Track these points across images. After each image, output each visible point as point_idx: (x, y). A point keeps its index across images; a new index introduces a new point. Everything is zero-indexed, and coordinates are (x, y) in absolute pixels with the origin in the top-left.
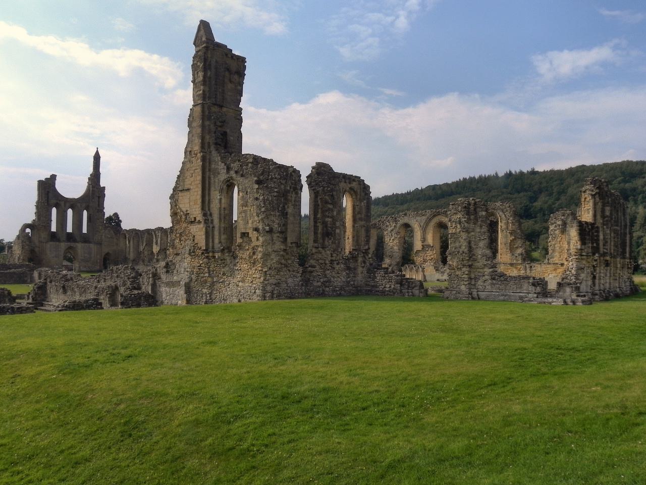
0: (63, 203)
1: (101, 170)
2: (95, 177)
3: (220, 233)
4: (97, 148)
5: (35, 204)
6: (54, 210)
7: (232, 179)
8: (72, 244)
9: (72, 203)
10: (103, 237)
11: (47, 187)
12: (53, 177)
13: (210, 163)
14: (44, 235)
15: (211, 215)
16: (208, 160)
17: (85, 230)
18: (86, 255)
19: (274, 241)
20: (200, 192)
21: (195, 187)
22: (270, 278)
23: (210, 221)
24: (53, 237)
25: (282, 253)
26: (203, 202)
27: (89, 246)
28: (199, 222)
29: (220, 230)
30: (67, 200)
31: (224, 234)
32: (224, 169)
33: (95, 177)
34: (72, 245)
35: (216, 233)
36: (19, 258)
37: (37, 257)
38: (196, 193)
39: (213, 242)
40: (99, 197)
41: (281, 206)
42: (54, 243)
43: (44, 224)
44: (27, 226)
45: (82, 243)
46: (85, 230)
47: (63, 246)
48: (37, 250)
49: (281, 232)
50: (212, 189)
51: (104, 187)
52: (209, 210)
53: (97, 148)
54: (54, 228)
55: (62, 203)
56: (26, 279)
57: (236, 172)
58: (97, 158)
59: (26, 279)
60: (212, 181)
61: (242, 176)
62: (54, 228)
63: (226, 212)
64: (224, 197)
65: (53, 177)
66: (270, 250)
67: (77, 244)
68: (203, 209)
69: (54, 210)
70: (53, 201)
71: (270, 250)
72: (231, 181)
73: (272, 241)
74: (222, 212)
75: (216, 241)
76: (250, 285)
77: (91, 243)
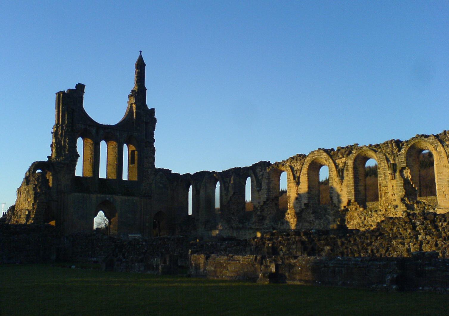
2: (139, 94)
4: (141, 52)
5: (52, 130)
8: (108, 197)
10: (153, 186)
11: (70, 102)
12: (80, 88)
33: (139, 94)
36: (28, 217)
40: (147, 123)
51: (153, 109)
53: (141, 52)
54: (79, 172)
58: (141, 66)
65: (80, 88)
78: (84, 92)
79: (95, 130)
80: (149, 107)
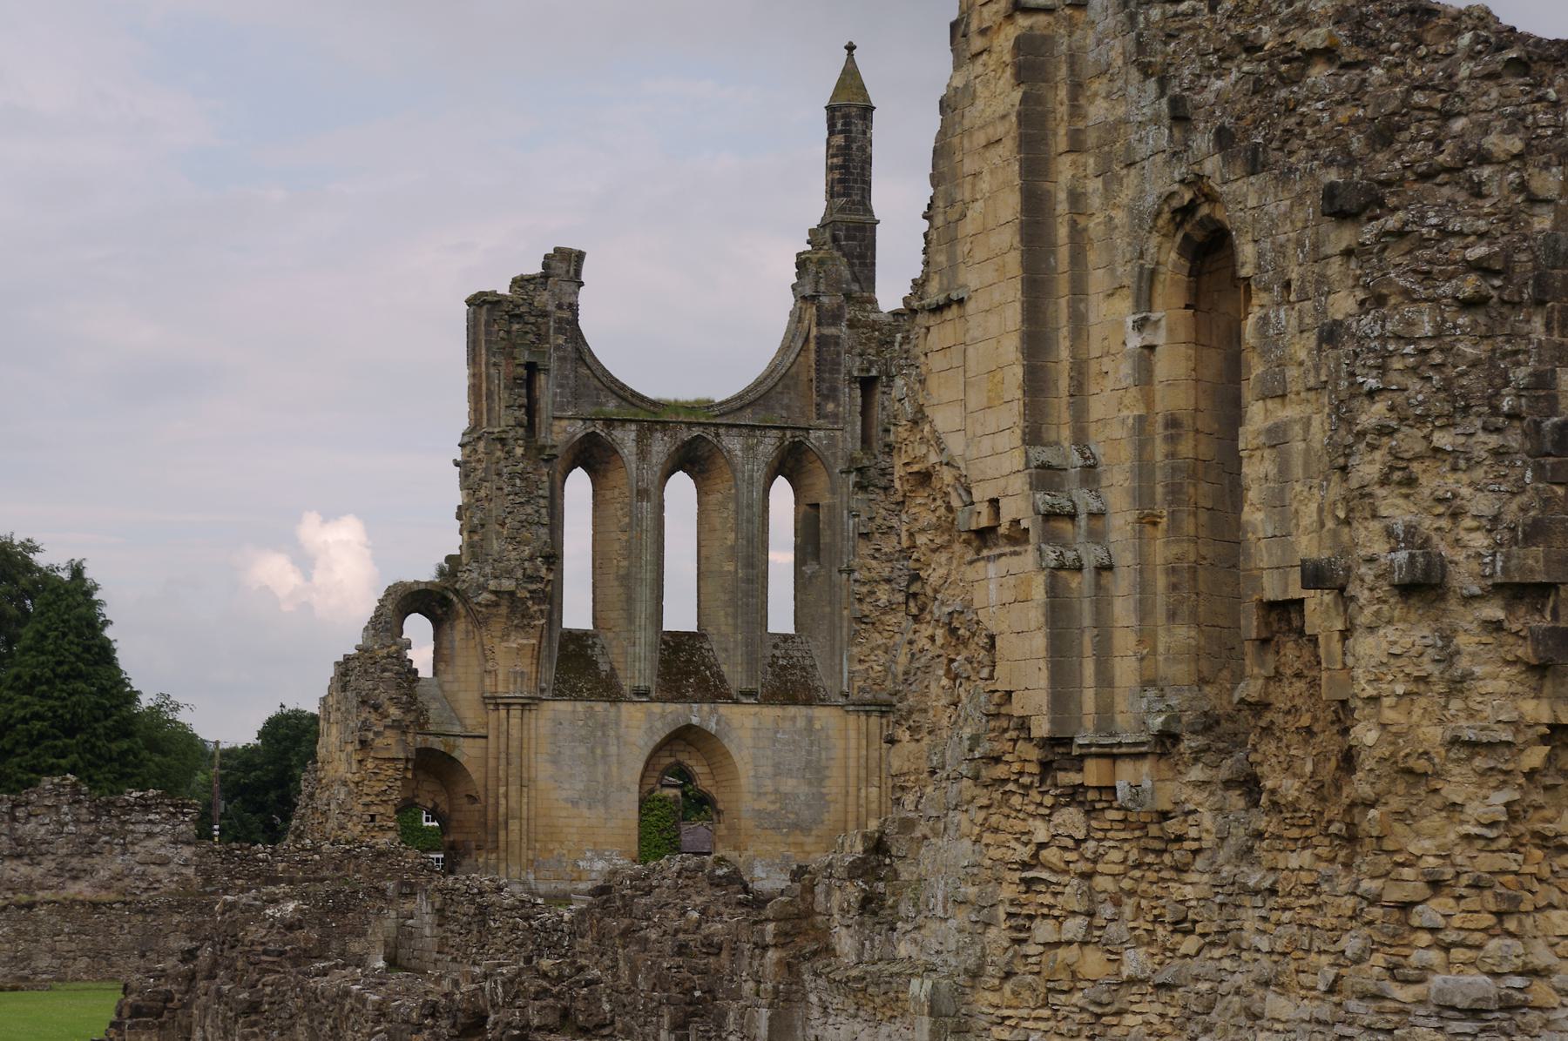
3: (1144, 611)
4: (851, 48)
6: (578, 485)
7: (1211, 198)
8: (699, 714)
9: (685, 435)
11: (526, 337)
12: (565, 266)
13: (1077, 88)
14: (510, 658)
15: (1090, 472)
16: (1063, 71)
17: (781, 617)
18: (788, 785)
19: (1463, 663)
20: (1013, 316)
21: (990, 275)
22: (1435, 956)
23: (1083, 520)
24: (577, 666)
25: (1535, 756)
26: (1036, 382)
27: (810, 720)
28: (1018, 536)
29: (1143, 587)
30: (651, 416)
31: (1172, 616)
32: (1156, 120)
34: (695, 720)
35: (1123, 611)
37: (473, 799)
38: (993, 320)
39: (1105, 679)
40: (867, 385)
41: (1521, 375)
42: (580, 706)
43: (507, 584)
44: (407, 600)
45: (768, 700)
46: (781, 617)
47: (640, 726)
48: (467, 752)
49: (1518, 592)
50: (1098, 280)
52: (1080, 439)
53: (851, 48)
54: (577, 613)
55: (626, 439)
56: (355, 947)
57: (1224, 139)
59: (355, 947)
60: (1094, 226)
61: (1255, 166)
63: (1186, 448)
64: (1171, 331)
65: (565, 266)
66: (1433, 735)
67: (724, 709)
68: (1033, 436)
69: (578, 485)
70: (562, 431)
71: (1433, 735)
72: (1205, 210)
73: (1448, 657)
74: (1160, 449)
75: (1125, 670)
76: (1325, 1011)
77: (824, 703)
78: (581, 284)
79: (633, 435)
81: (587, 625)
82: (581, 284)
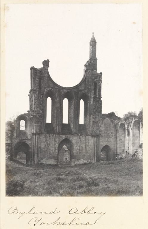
0: (58, 93)
1: (98, 56)
4: (93, 33)
6: (49, 100)
24: (49, 129)
46: (82, 121)
51: (101, 73)
53: (93, 33)
54: (49, 120)
58: (93, 43)
62: (49, 120)
69: (49, 100)
80: (99, 71)
81: (50, 122)
82: (49, 66)
